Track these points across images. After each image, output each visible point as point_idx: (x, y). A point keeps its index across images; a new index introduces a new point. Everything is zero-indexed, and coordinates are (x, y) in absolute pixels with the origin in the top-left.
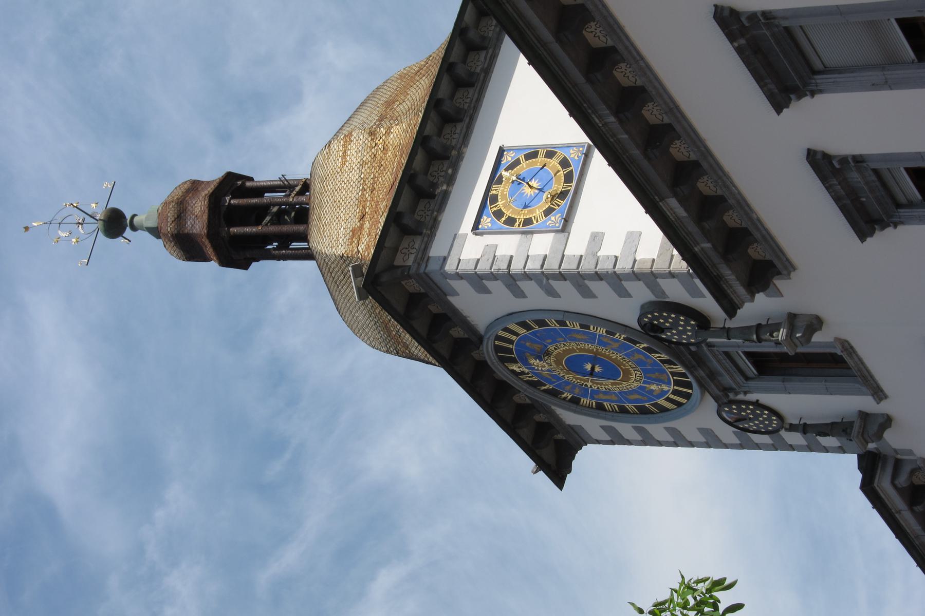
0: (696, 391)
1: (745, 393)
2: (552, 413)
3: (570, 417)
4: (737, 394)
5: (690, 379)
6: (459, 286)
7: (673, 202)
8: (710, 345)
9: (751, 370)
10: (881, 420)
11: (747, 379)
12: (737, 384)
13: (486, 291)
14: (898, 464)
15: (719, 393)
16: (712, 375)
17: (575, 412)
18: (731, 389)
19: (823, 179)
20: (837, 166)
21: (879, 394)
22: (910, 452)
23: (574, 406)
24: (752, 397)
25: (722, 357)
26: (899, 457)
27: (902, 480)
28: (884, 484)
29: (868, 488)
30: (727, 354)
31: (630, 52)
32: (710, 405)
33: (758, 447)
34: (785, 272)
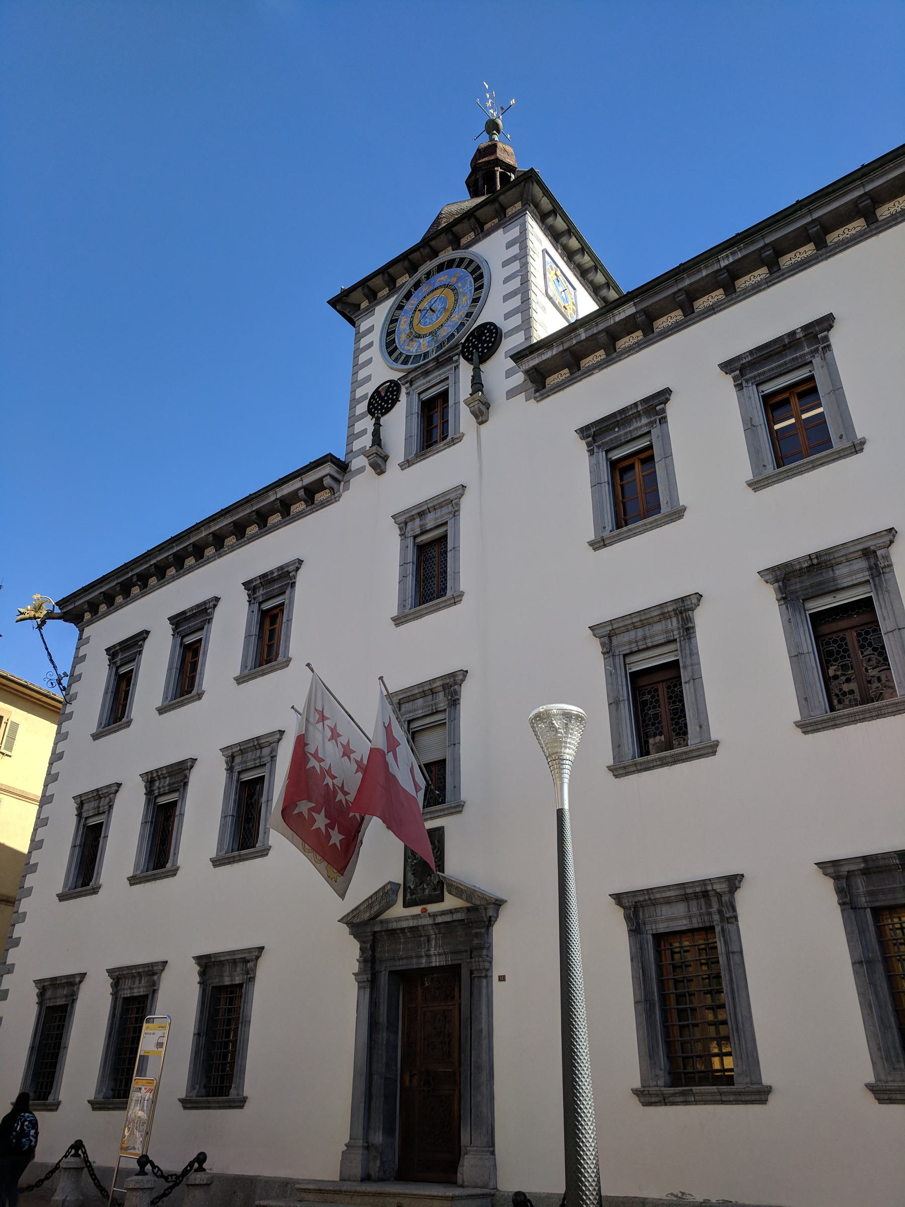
0: (409, 366)
1: (408, 394)
2: (388, 297)
3: (383, 310)
4: (407, 388)
5: (421, 363)
6: (514, 232)
7: (632, 310)
8: (457, 367)
9: (425, 396)
10: (383, 467)
11: (419, 394)
12: (417, 388)
13: (509, 245)
14: (338, 481)
15: (409, 378)
16: (426, 373)
17: (391, 307)
18: (411, 385)
19: (645, 401)
20: (658, 408)
21: (407, 464)
22: (347, 488)
23: (395, 307)
24: (403, 397)
25: (443, 377)
26: (342, 483)
27: (327, 481)
28: (327, 469)
29: (329, 458)
30: (447, 378)
31: (778, 277)
32: (396, 376)
33: (352, 408)
34: (538, 394)
